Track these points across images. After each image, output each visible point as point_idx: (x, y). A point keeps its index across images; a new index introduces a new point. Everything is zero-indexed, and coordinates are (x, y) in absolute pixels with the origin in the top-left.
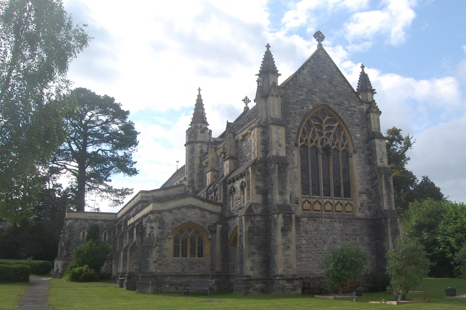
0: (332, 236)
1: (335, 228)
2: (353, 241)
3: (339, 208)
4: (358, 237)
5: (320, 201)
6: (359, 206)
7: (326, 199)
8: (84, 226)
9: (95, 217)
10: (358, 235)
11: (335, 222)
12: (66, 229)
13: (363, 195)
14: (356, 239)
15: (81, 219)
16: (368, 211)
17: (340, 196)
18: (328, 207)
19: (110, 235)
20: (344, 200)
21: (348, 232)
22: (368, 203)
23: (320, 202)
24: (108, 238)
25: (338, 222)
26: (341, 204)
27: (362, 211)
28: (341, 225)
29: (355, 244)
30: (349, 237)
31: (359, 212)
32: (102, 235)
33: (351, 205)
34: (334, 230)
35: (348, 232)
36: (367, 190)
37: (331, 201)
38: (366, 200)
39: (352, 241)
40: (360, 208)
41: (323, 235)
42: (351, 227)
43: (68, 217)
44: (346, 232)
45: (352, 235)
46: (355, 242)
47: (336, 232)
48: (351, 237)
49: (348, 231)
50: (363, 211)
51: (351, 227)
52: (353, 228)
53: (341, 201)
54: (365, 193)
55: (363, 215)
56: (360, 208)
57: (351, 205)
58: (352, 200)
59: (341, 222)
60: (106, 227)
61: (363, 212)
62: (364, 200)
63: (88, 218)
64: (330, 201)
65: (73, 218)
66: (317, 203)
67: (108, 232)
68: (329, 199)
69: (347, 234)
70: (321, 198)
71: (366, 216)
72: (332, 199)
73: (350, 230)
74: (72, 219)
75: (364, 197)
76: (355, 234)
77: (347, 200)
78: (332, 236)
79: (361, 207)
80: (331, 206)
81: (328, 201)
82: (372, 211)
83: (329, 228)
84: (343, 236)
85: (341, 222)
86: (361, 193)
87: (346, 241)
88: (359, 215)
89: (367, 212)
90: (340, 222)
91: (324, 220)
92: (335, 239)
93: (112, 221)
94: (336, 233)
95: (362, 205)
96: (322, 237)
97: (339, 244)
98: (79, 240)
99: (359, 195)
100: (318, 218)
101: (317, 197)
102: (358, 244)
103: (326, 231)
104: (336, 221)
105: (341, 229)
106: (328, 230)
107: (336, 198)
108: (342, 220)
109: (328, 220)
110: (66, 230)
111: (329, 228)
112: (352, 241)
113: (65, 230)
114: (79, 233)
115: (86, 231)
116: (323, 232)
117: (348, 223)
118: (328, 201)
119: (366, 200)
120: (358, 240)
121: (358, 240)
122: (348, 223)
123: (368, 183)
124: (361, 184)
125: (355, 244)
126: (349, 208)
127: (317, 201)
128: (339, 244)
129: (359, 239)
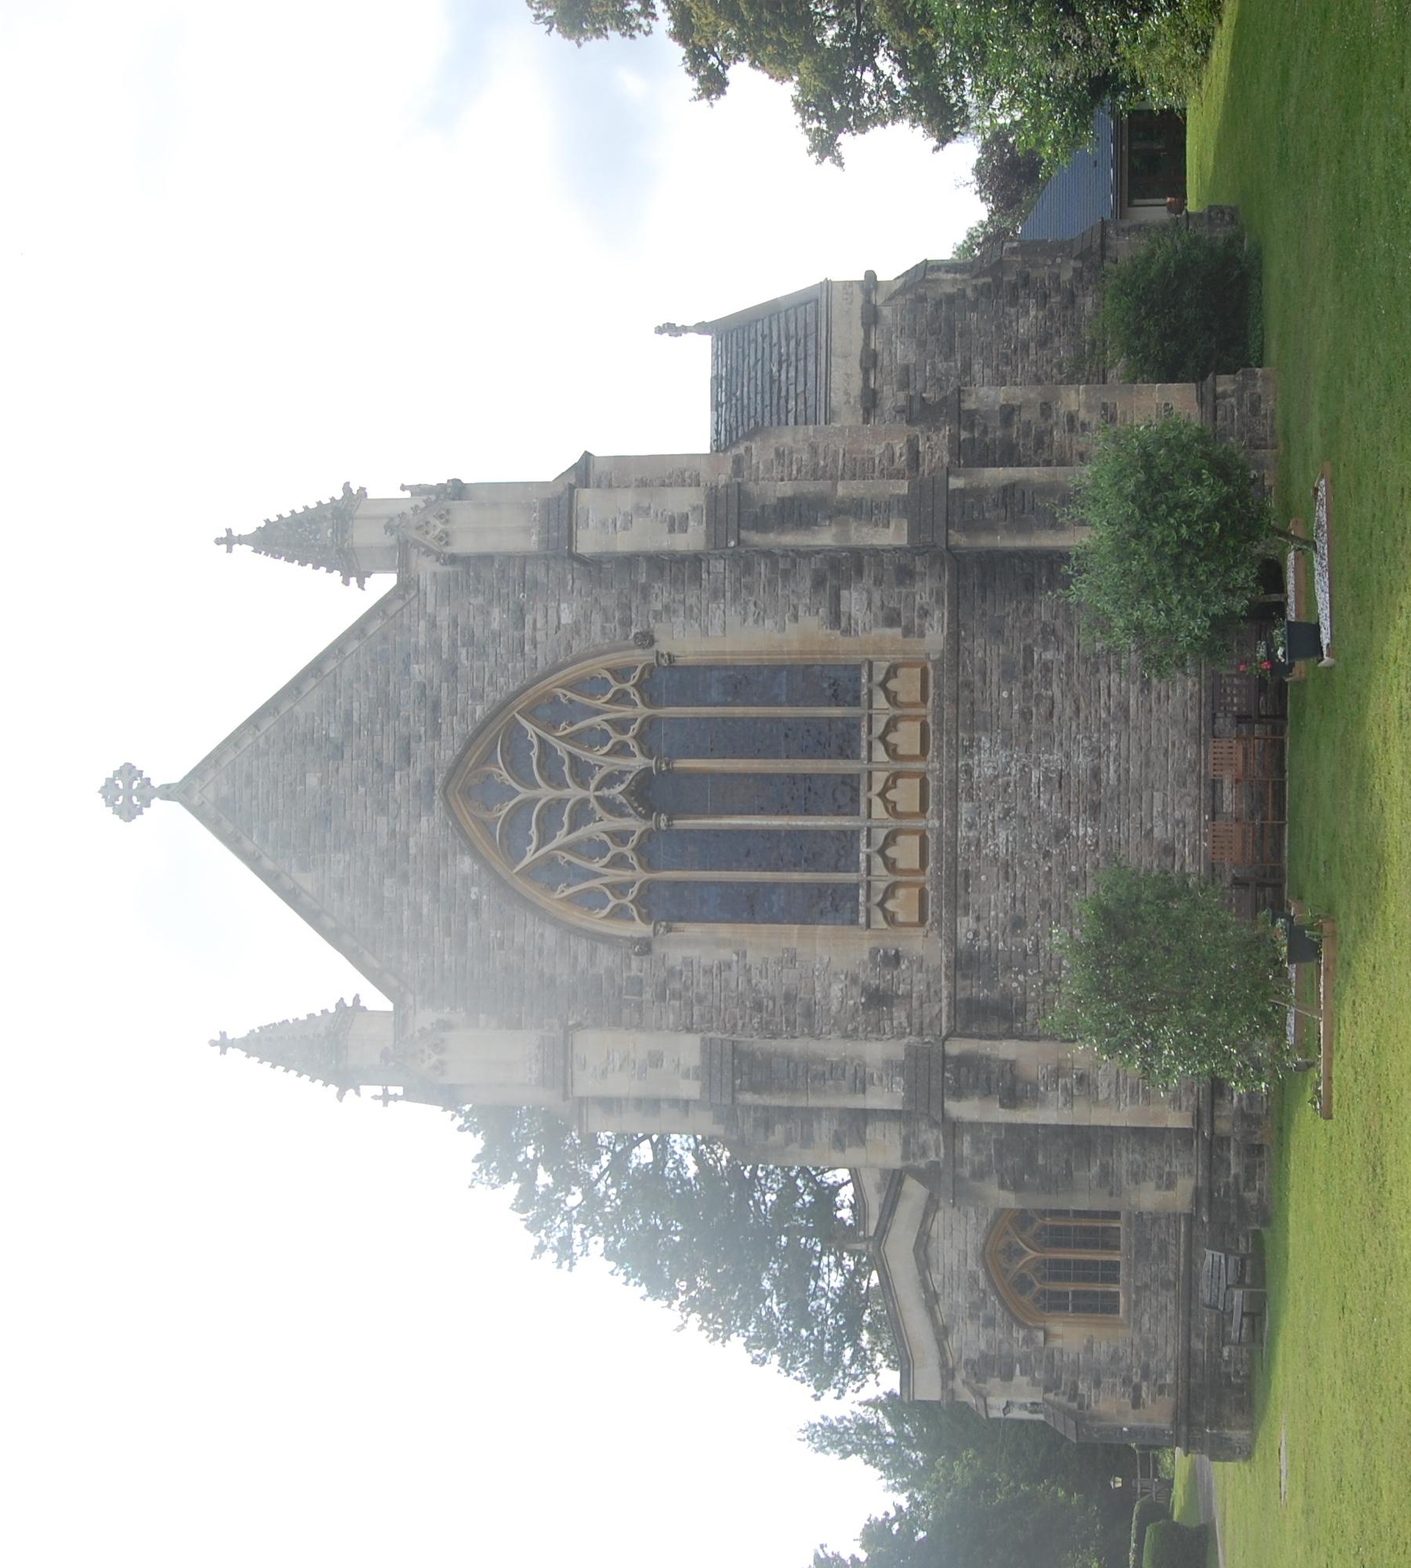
0: (1034, 796)
1: (996, 777)
2: (1055, 685)
3: (907, 738)
4: (1036, 657)
5: (880, 836)
6: (897, 631)
7: (870, 801)
10: (1028, 651)
11: (971, 776)
13: (843, 608)
14: (1047, 668)
16: (919, 585)
17: (853, 725)
18: (906, 795)
20: (870, 707)
21: (1016, 707)
22: (878, 582)
23: (886, 838)
25: (971, 756)
26: (891, 725)
27: (917, 621)
28: (985, 742)
29: (1069, 675)
30: (1037, 705)
31: (922, 635)
33: (892, 672)
34: (1008, 784)
35: (1016, 707)
36: (819, 582)
37: (879, 779)
38: (869, 592)
39: (1056, 690)
40: (908, 632)
41: (1030, 842)
42: (994, 688)
44: (1016, 717)
45: (1027, 685)
46: (1060, 671)
47: (1014, 769)
48: (1039, 695)
49: (1011, 705)
50: (920, 617)
51: (994, 688)
52: (995, 679)
53: (879, 728)
54: (836, 599)
55: (937, 614)
56: (908, 632)
57: (892, 672)
58: (871, 663)
59: (972, 740)
61: (925, 613)
62: (869, 605)
64: (877, 787)
66: (891, 852)
68: (870, 788)
69: (1026, 715)
70: (869, 830)
71: (939, 600)
72: (870, 773)
73: (1005, 694)
75: (853, 601)
76: (1026, 670)
77: (870, 693)
78: (1034, 796)
79: (899, 625)
80: (900, 782)
81: (882, 795)
82: (919, 568)
83: (999, 807)
84: (1032, 736)
85: (972, 740)
86: (835, 618)
87: (1055, 720)
88: (935, 638)
89: (923, 592)
90: (971, 746)
91: (963, 831)
92: (1048, 780)
94: (1022, 770)
95: (892, 620)
96: (1039, 848)
97: (1068, 756)
99: (847, 632)
100: (955, 859)
101: (863, 848)
102: (1069, 657)
103: (1014, 822)
104: (969, 771)
105: (1006, 744)
106: (1007, 812)
107: (864, 754)
108: (961, 734)
109: (965, 807)
111: (999, 807)
112: (1056, 690)
116: (1014, 839)
117: (972, 704)
118: (882, 795)
119: (865, 595)
120: (1049, 655)
121: (1049, 655)
122: (972, 704)
123: (786, 574)
124: (796, 618)
125: (1069, 675)
126: (907, 685)
127: (881, 852)
128: (1068, 756)
129: (1046, 649)
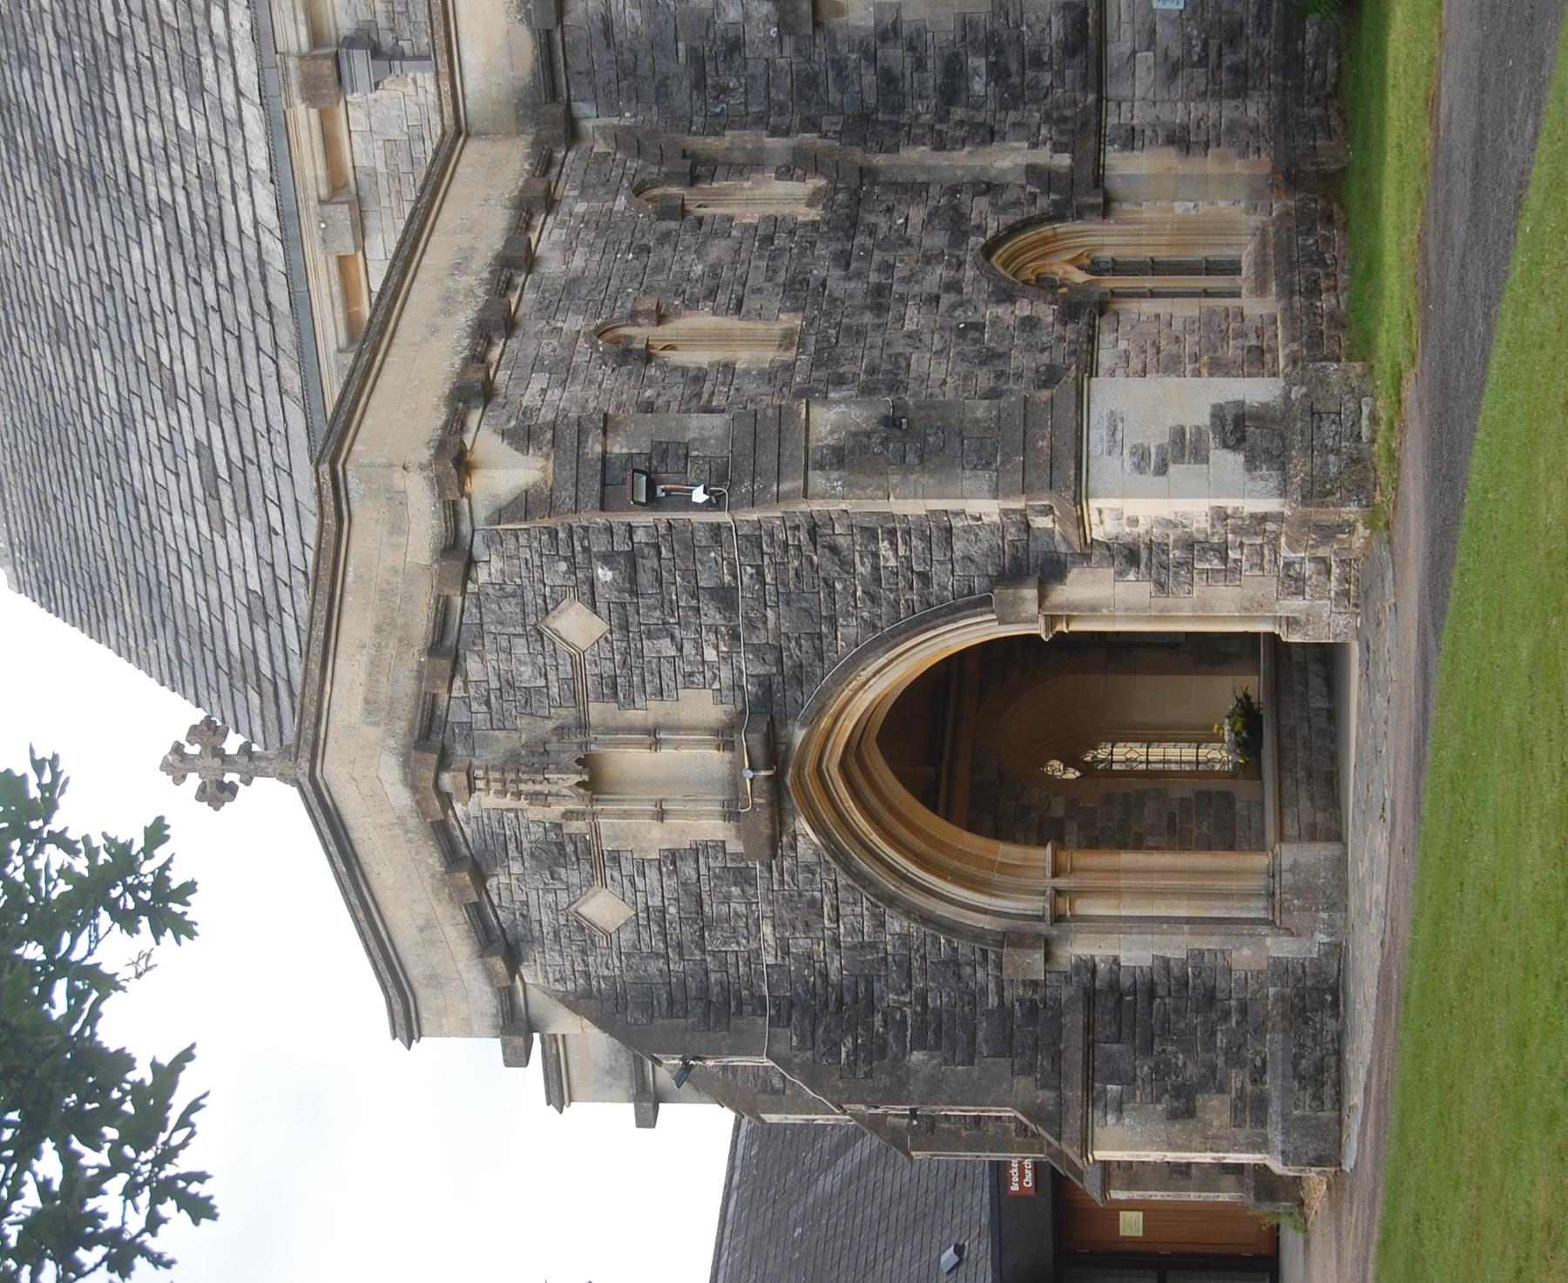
8: (582, 344)
9: (458, 267)
12: (594, 448)
15: (477, 358)
19: (752, 164)
24: (785, 173)
32: (730, 219)
43: (426, 455)
60: (621, 202)
63: (466, 315)
65: (437, 418)
67: (694, 180)
74: (456, 424)
93: (544, 163)
98: (789, 367)
110: (618, 448)
113: (604, 458)
114: (684, 370)
115: (660, 318)
